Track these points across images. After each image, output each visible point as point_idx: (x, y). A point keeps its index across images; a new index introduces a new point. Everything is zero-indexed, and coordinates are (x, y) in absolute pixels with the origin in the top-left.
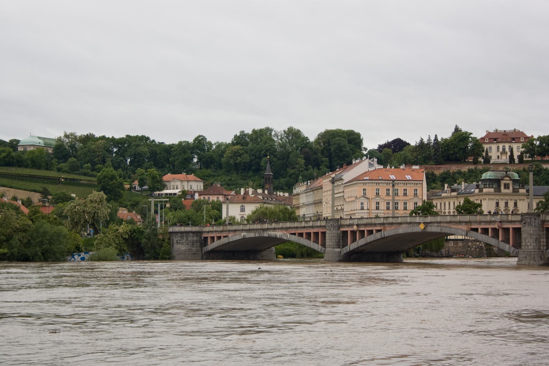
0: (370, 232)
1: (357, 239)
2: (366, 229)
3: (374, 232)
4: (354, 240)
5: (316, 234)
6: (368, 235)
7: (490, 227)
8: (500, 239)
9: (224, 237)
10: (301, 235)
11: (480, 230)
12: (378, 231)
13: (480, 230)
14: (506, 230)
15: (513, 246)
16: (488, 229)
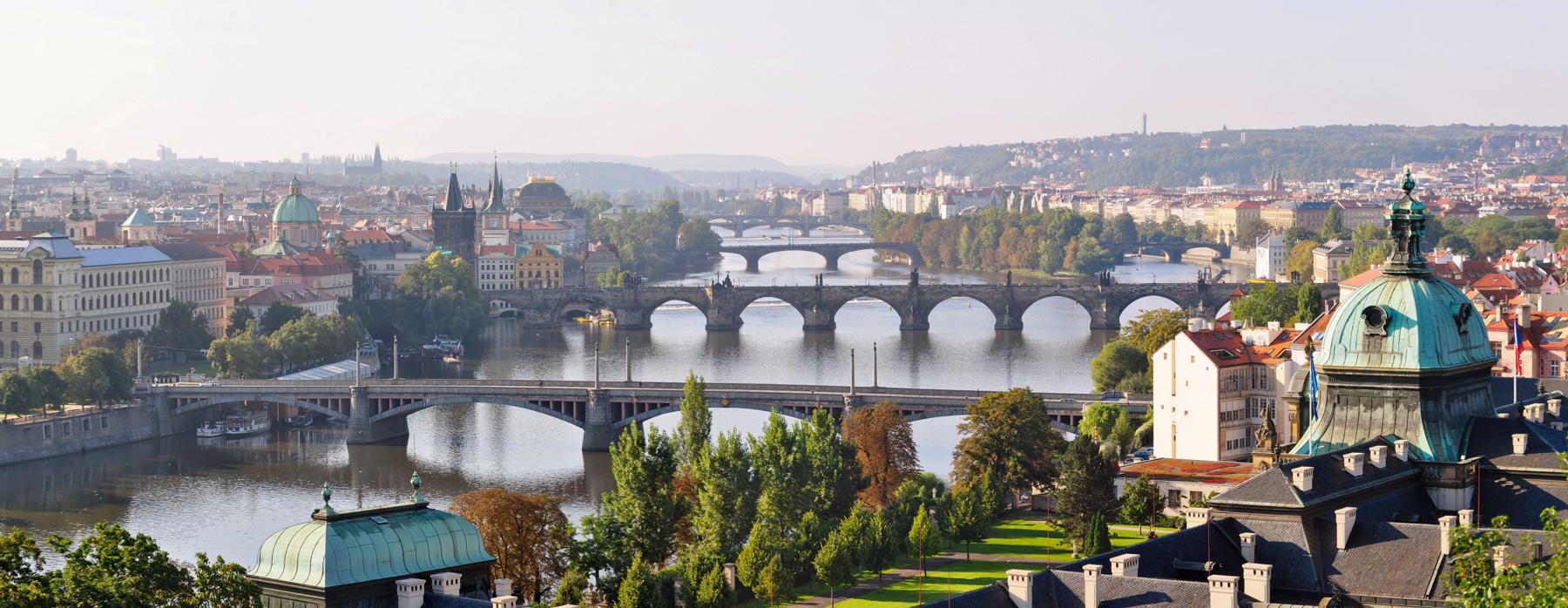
0: (407, 401)
1: (390, 407)
2: (401, 397)
3: (412, 401)
4: (386, 408)
5: (335, 402)
6: (404, 404)
7: (551, 400)
8: (563, 411)
9: (202, 399)
10: (314, 401)
11: (540, 403)
12: (416, 400)
13: (540, 403)
14: (569, 405)
15: (577, 419)
16: (549, 402)
